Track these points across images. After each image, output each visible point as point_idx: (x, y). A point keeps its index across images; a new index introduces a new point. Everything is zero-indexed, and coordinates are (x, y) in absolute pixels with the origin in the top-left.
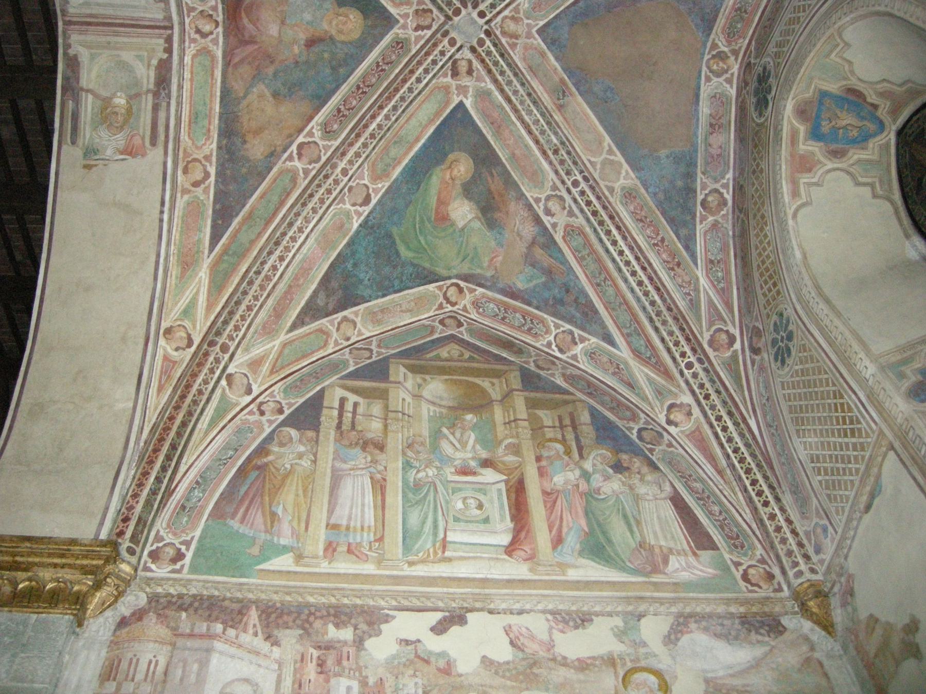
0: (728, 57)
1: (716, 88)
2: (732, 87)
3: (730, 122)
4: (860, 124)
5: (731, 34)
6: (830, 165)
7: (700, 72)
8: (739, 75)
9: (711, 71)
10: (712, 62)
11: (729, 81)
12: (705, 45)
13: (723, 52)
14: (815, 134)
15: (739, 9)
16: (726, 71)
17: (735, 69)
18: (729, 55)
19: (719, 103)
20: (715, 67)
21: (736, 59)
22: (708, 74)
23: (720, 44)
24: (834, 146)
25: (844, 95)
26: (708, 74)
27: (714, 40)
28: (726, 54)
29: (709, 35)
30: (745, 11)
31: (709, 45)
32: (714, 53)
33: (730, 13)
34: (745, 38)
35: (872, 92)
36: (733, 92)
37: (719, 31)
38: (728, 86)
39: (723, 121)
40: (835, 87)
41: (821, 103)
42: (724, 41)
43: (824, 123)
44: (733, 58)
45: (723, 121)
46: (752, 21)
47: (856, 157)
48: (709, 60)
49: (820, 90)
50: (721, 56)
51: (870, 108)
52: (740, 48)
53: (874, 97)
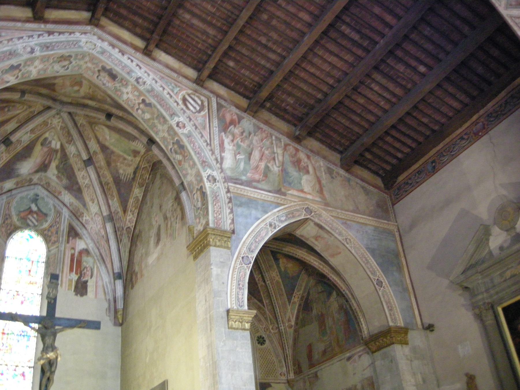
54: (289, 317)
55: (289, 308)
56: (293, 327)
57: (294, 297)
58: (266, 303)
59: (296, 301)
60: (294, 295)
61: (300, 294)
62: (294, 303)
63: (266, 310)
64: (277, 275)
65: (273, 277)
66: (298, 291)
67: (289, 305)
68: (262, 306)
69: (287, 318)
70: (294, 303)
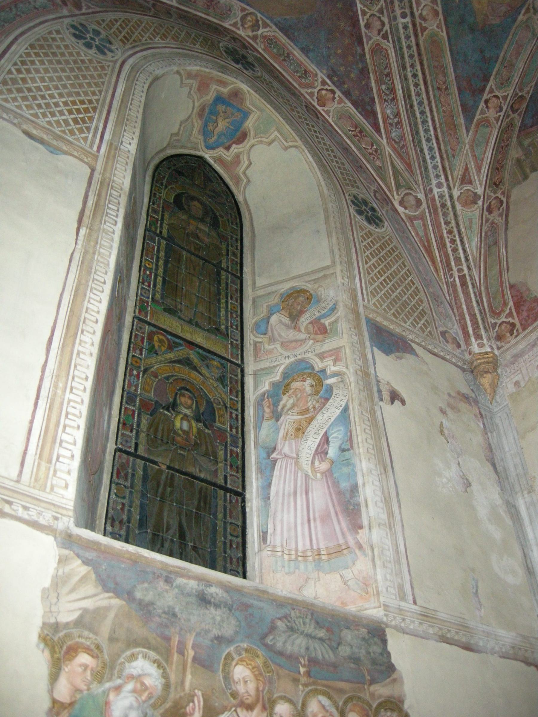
0: (253, 31)
1: (235, 14)
2: (230, 25)
3: (208, 15)
4: (215, 133)
5: (270, 41)
6: (197, 104)
7: (251, 6)
8: (236, 33)
9: (247, 15)
10: (254, 18)
11: (235, 25)
12: (268, 18)
13: (258, 30)
14: (219, 99)
15: (288, 56)
16: (242, 25)
17: (241, 32)
18: (254, 33)
19: (224, 12)
20: (249, 18)
21: (249, 36)
22: (247, 12)
23: (265, 30)
24: (207, 110)
25: (242, 129)
26: (247, 12)
27: (271, 27)
28: (255, 31)
29: (276, 25)
30: (285, 60)
31: (268, 22)
32: (260, 23)
33: (288, 49)
34: (264, 50)
35: (240, 150)
36: (226, 25)
37: (277, 35)
38: (232, 23)
39: (211, 10)
40: (250, 125)
41: (239, 110)
42: (267, 34)
43: (224, 107)
44: (251, 34)
45: (211, 10)
46: (275, 62)
47: (196, 124)
48: (257, 17)
49: (250, 113)
50: (255, 26)
51: (227, 145)
52: (257, 44)
53: (236, 150)
54: (467, 169)
55: (467, 139)
56: (480, 203)
57: (487, 102)
58: (385, 118)
59: (493, 120)
60: (485, 96)
61: (505, 98)
62: (485, 123)
63: (384, 142)
64: (437, 14)
65: (421, 16)
66: (504, 83)
67: (468, 131)
68: (368, 127)
69: (458, 173)
70: (485, 123)
